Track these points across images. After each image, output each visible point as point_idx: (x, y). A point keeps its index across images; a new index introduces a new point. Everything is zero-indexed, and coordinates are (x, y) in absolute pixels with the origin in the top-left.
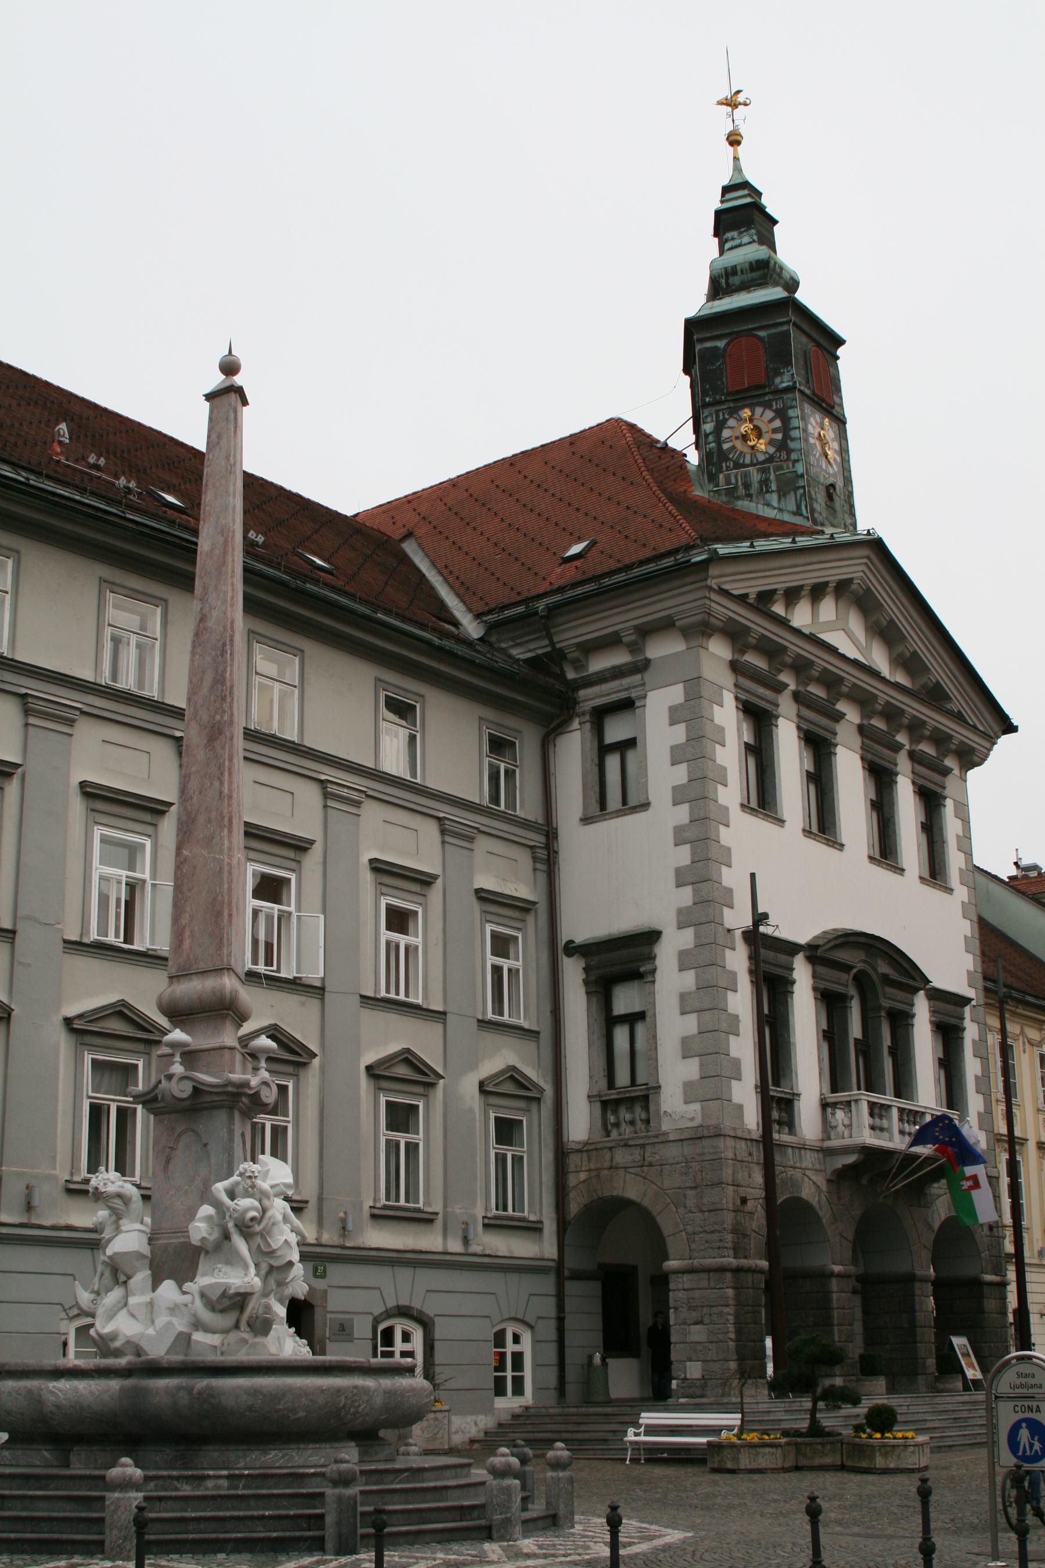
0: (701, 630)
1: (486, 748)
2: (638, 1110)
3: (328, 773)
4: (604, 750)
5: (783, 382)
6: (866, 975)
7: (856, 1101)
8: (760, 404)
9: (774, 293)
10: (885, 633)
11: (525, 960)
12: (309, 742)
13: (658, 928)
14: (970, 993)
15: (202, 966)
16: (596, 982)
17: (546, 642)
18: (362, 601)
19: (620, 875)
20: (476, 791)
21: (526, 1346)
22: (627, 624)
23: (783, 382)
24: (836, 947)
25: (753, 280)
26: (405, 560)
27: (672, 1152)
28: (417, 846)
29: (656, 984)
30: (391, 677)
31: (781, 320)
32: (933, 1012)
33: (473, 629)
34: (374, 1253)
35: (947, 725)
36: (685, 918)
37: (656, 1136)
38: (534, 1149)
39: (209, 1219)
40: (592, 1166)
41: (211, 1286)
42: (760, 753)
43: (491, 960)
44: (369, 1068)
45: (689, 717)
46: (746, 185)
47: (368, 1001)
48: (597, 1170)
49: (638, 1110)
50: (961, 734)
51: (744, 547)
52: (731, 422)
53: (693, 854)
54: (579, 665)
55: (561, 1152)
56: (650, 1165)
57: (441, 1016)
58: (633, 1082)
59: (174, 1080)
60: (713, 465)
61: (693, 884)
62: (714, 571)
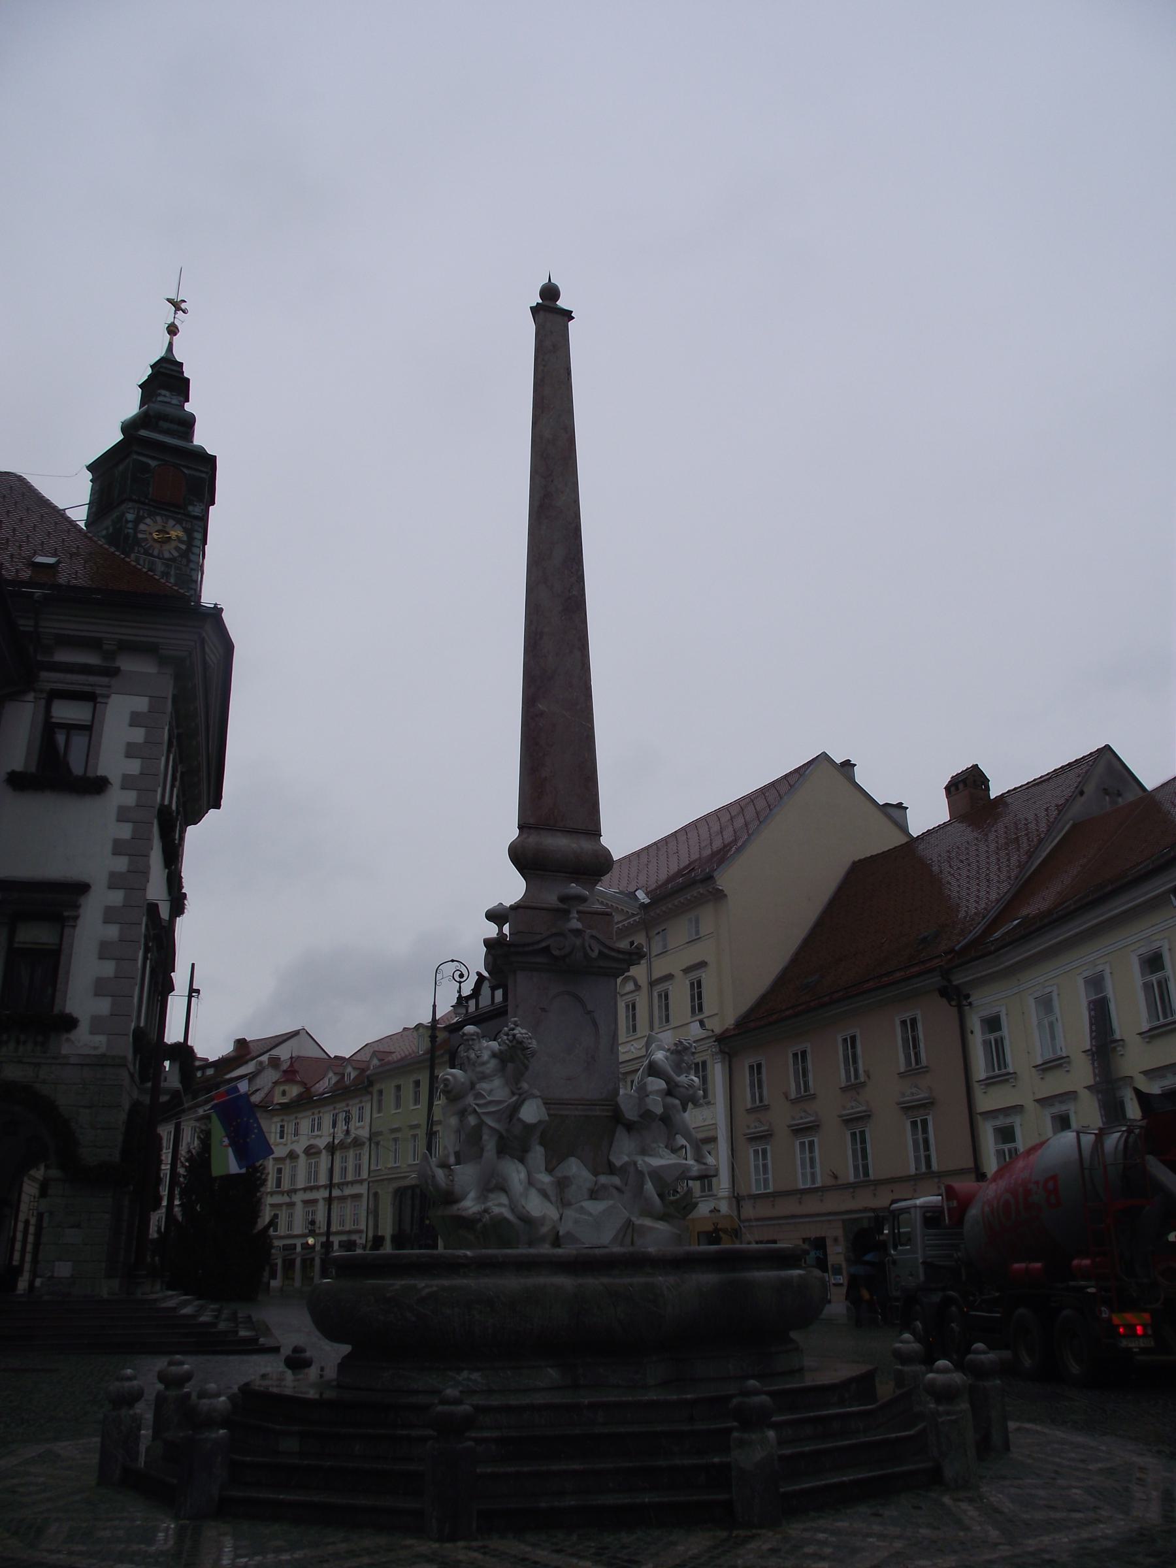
8: (174, 519)
29: (78, 929)
36: (115, 881)
41: (668, 1166)
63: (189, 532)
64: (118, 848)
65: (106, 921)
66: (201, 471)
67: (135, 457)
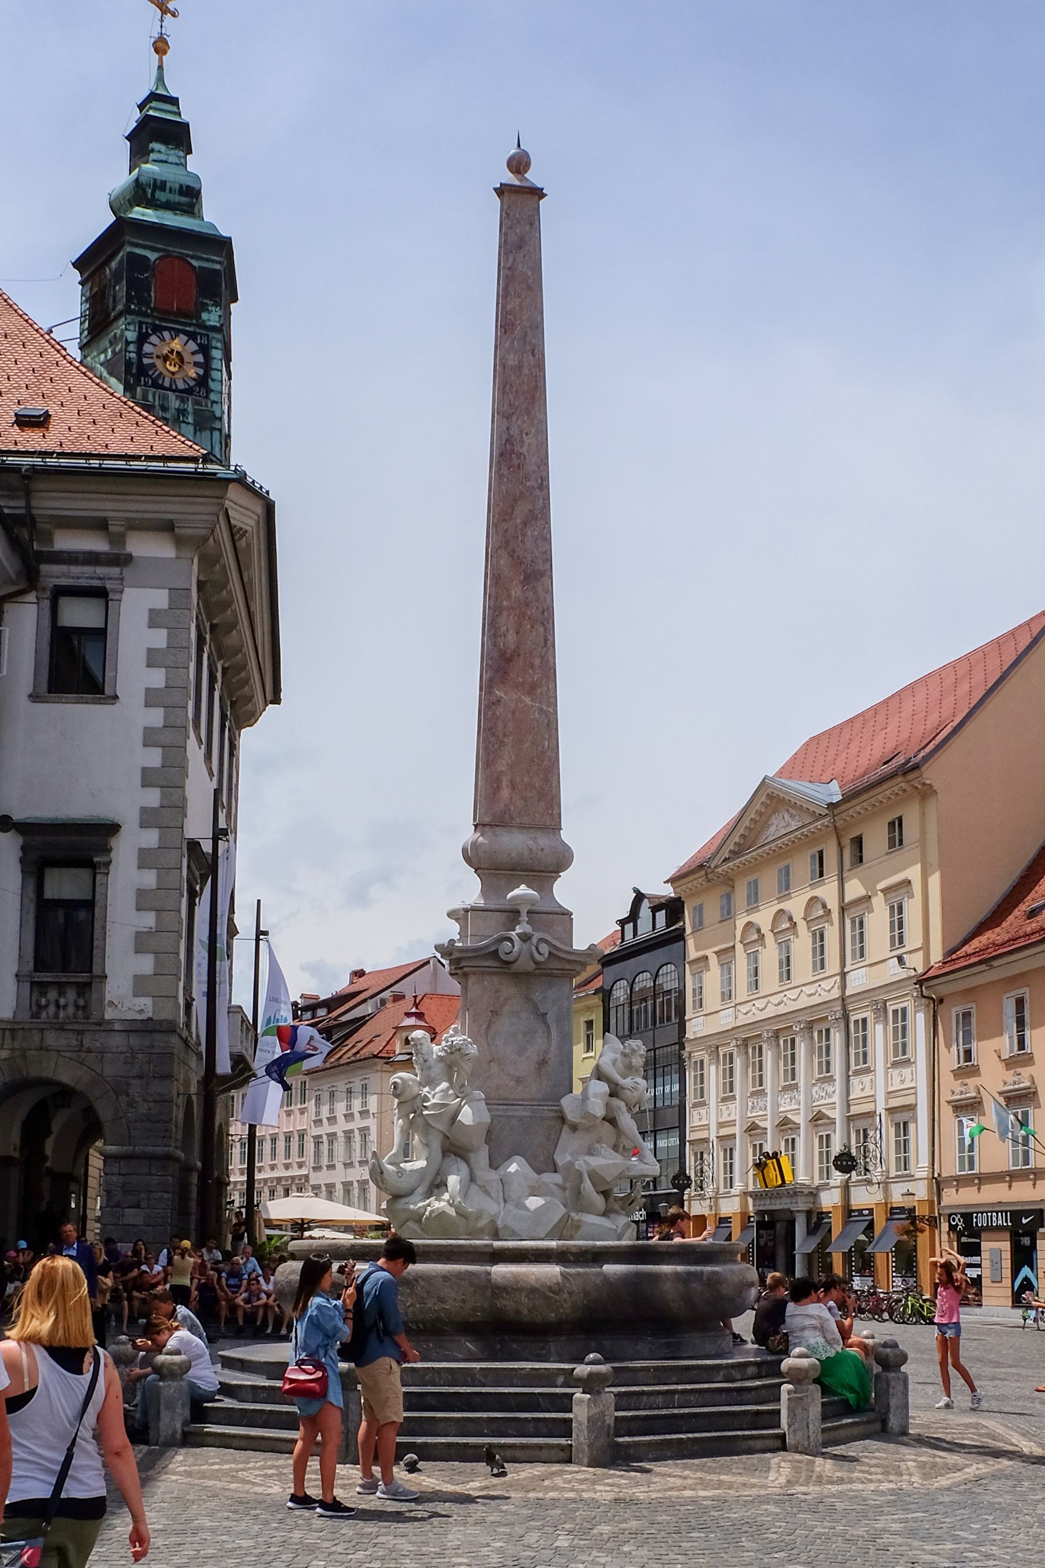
8: (185, 333)
13: (117, 819)
17: (22, 503)
25: (179, 203)
31: (215, 258)
45: (172, 625)
46: (174, 101)
52: (154, 339)
60: (132, 375)
61: (162, 787)
63: (205, 350)
64: (148, 778)
66: (213, 261)
67: (128, 249)
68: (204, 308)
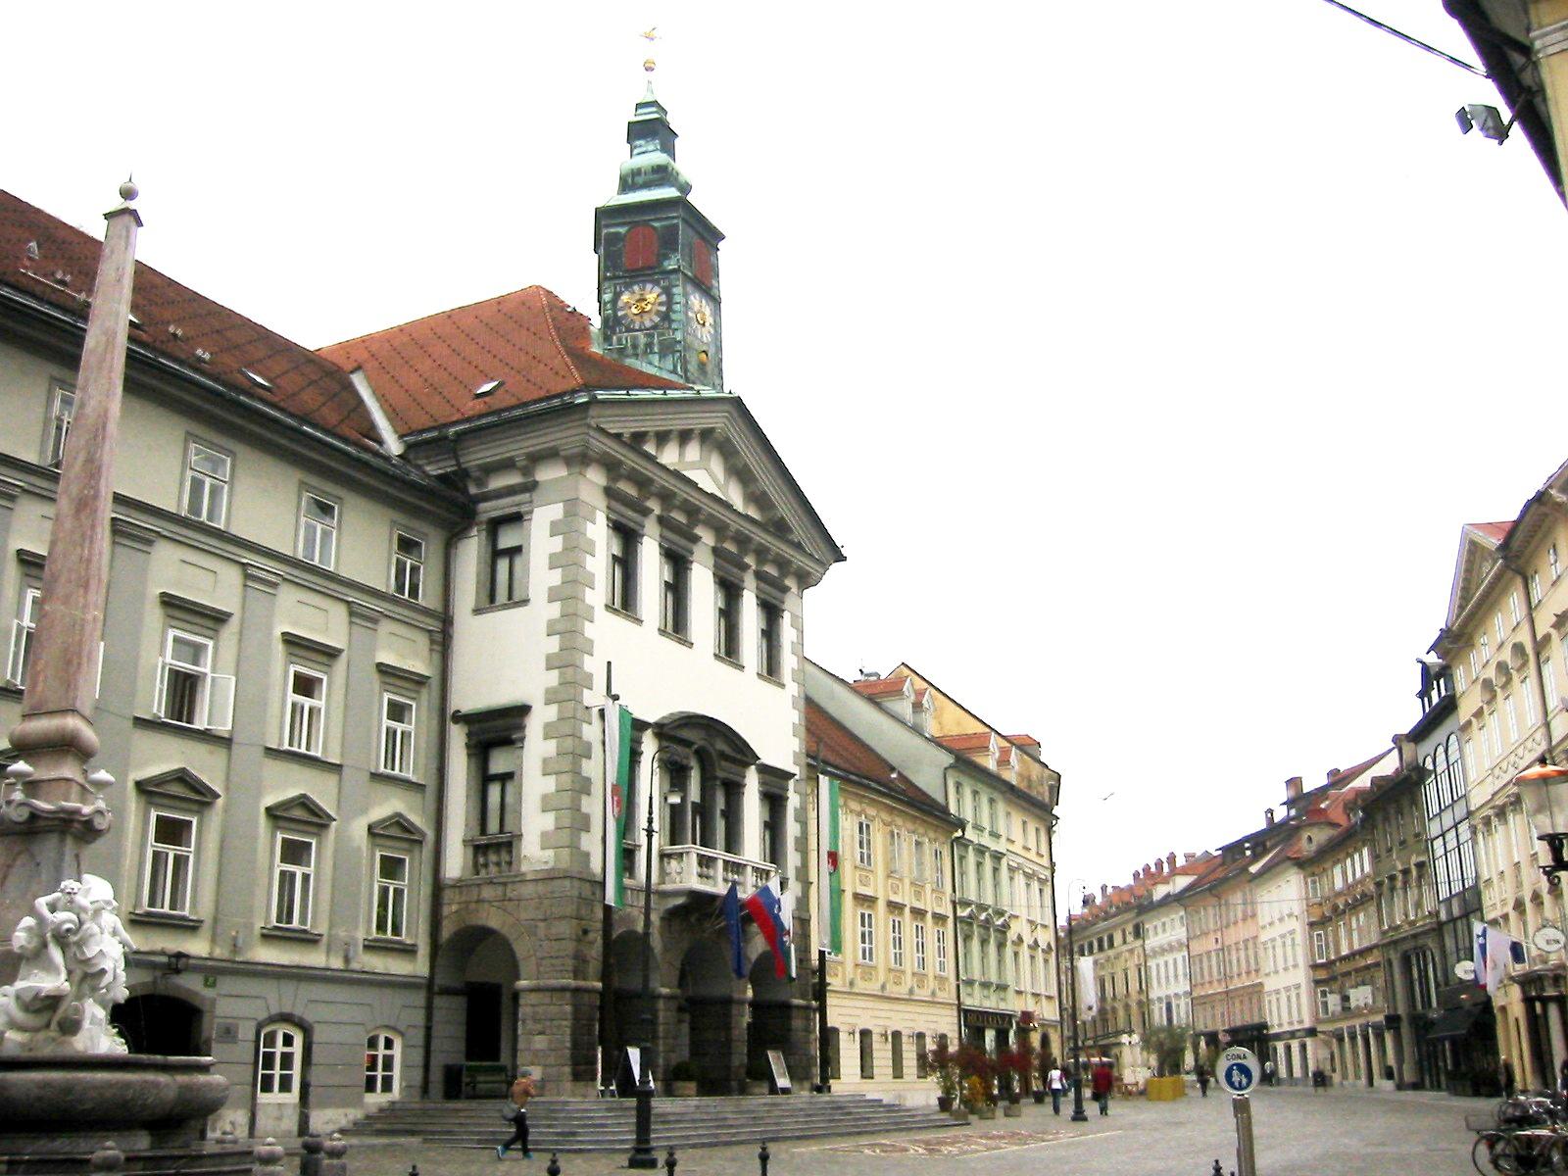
0: (580, 460)
1: (395, 547)
2: (505, 857)
3: (248, 558)
4: (496, 554)
5: (670, 265)
6: (703, 751)
7: (688, 853)
9: (669, 192)
10: (740, 473)
11: (417, 725)
12: (234, 531)
13: (529, 703)
14: (795, 770)
15: (52, 707)
16: (476, 746)
17: (454, 462)
18: (291, 415)
19: (502, 658)
20: (385, 582)
21: (397, 1051)
22: (523, 451)
23: (670, 265)
24: (680, 726)
26: (350, 387)
27: (528, 890)
28: (328, 625)
30: (314, 481)
32: (762, 783)
33: (394, 446)
34: (260, 967)
35: (788, 552)
37: (516, 876)
38: (414, 885)
39: (29, 929)
40: (464, 899)
42: (626, 563)
43: (386, 723)
44: (268, 810)
46: (655, 103)
47: (270, 752)
48: (467, 903)
49: (505, 857)
50: (799, 560)
51: (621, 394)
53: (562, 642)
54: (480, 483)
55: (438, 887)
56: (510, 900)
57: (337, 768)
58: (501, 831)
59: (13, 806)
62: (593, 411)
65: (546, 737)
66: (674, 218)
67: (604, 231)
68: (667, 257)
